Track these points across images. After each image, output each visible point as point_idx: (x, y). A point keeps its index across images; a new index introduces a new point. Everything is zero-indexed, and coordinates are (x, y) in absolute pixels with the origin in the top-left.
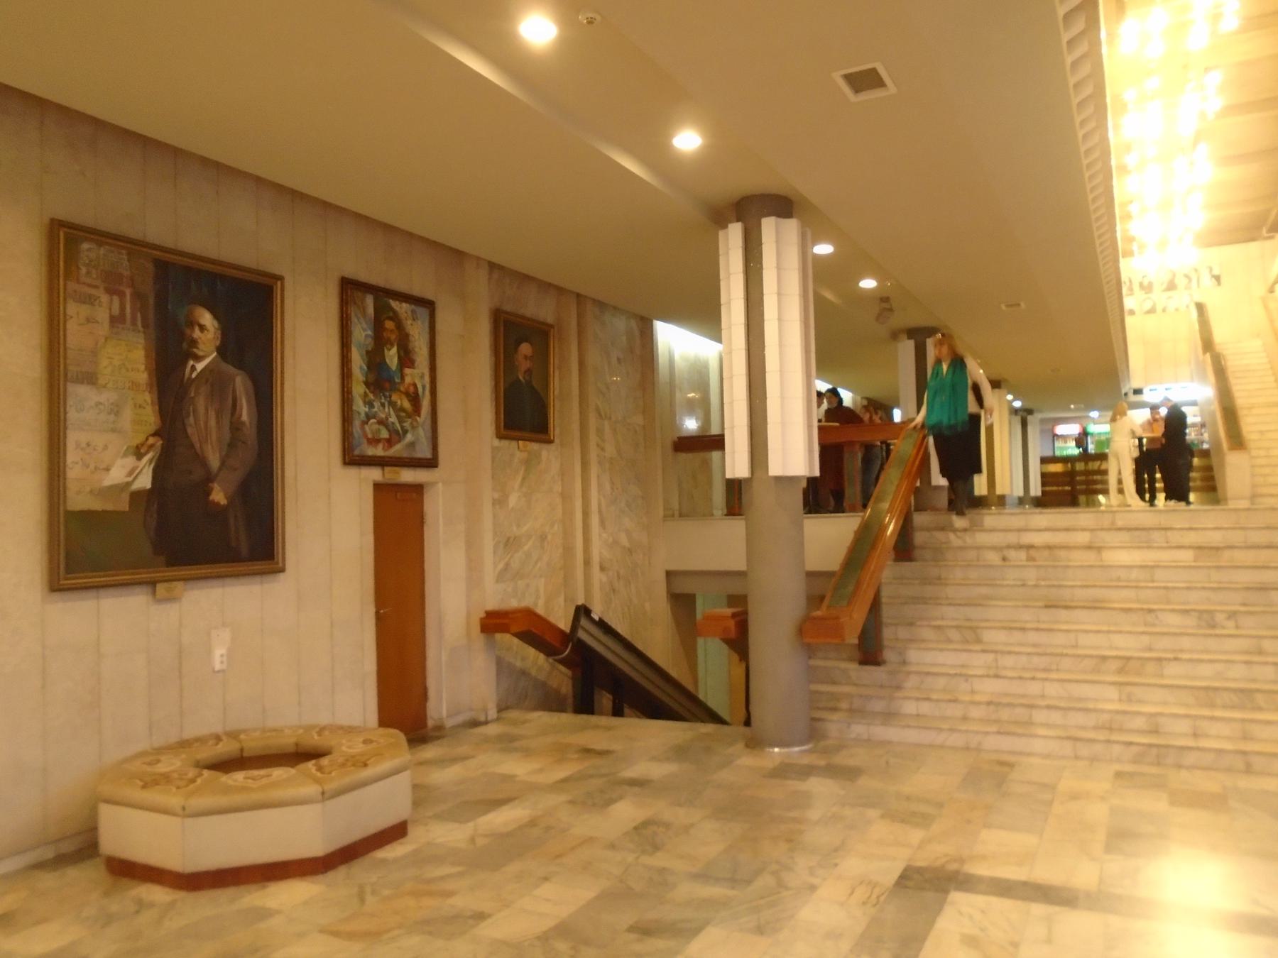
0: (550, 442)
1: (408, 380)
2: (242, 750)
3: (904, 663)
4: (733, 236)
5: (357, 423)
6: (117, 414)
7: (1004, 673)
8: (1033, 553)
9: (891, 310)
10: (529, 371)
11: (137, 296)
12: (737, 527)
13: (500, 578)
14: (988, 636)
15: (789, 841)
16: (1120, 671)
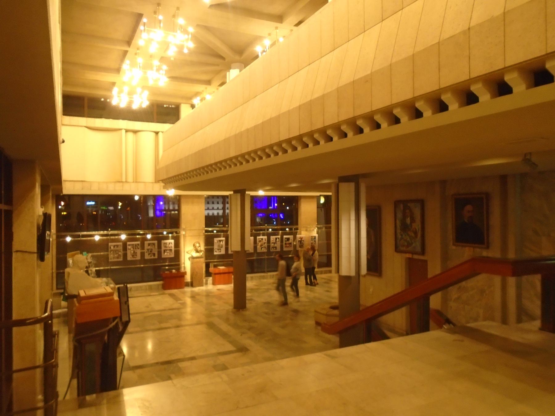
1: (413, 227)
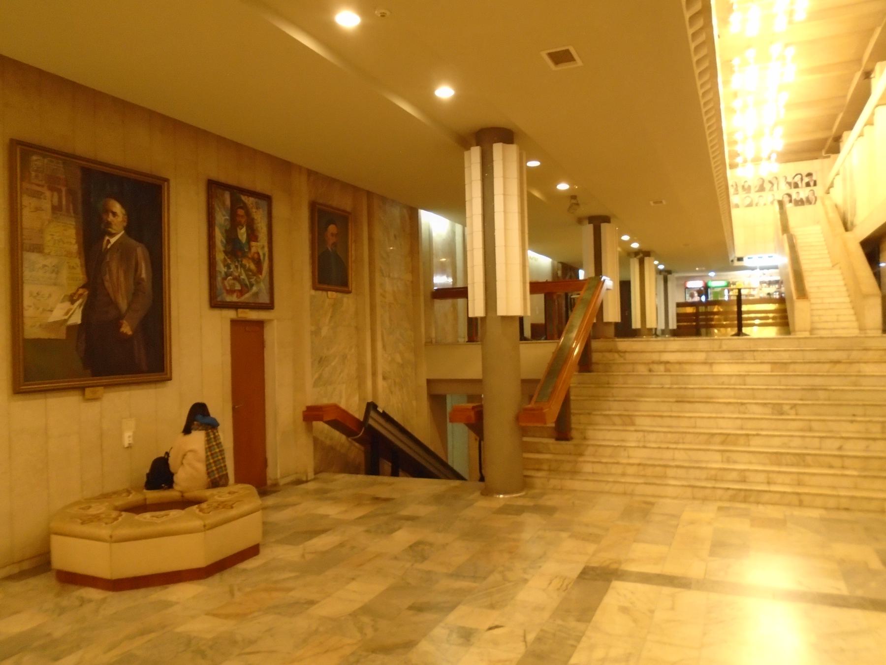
0: (349, 292)
1: (253, 250)
2: (145, 499)
3: (585, 438)
4: (474, 155)
5: (219, 279)
6: (57, 273)
7: (648, 445)
8: (668, 366)
9: (578, 204)
10: (334, 244)
11: (70, 192)
12: (475, 350)
13: (315, 385)
14: (638, 421)
15: (511, 552)
16: (723, 443)
